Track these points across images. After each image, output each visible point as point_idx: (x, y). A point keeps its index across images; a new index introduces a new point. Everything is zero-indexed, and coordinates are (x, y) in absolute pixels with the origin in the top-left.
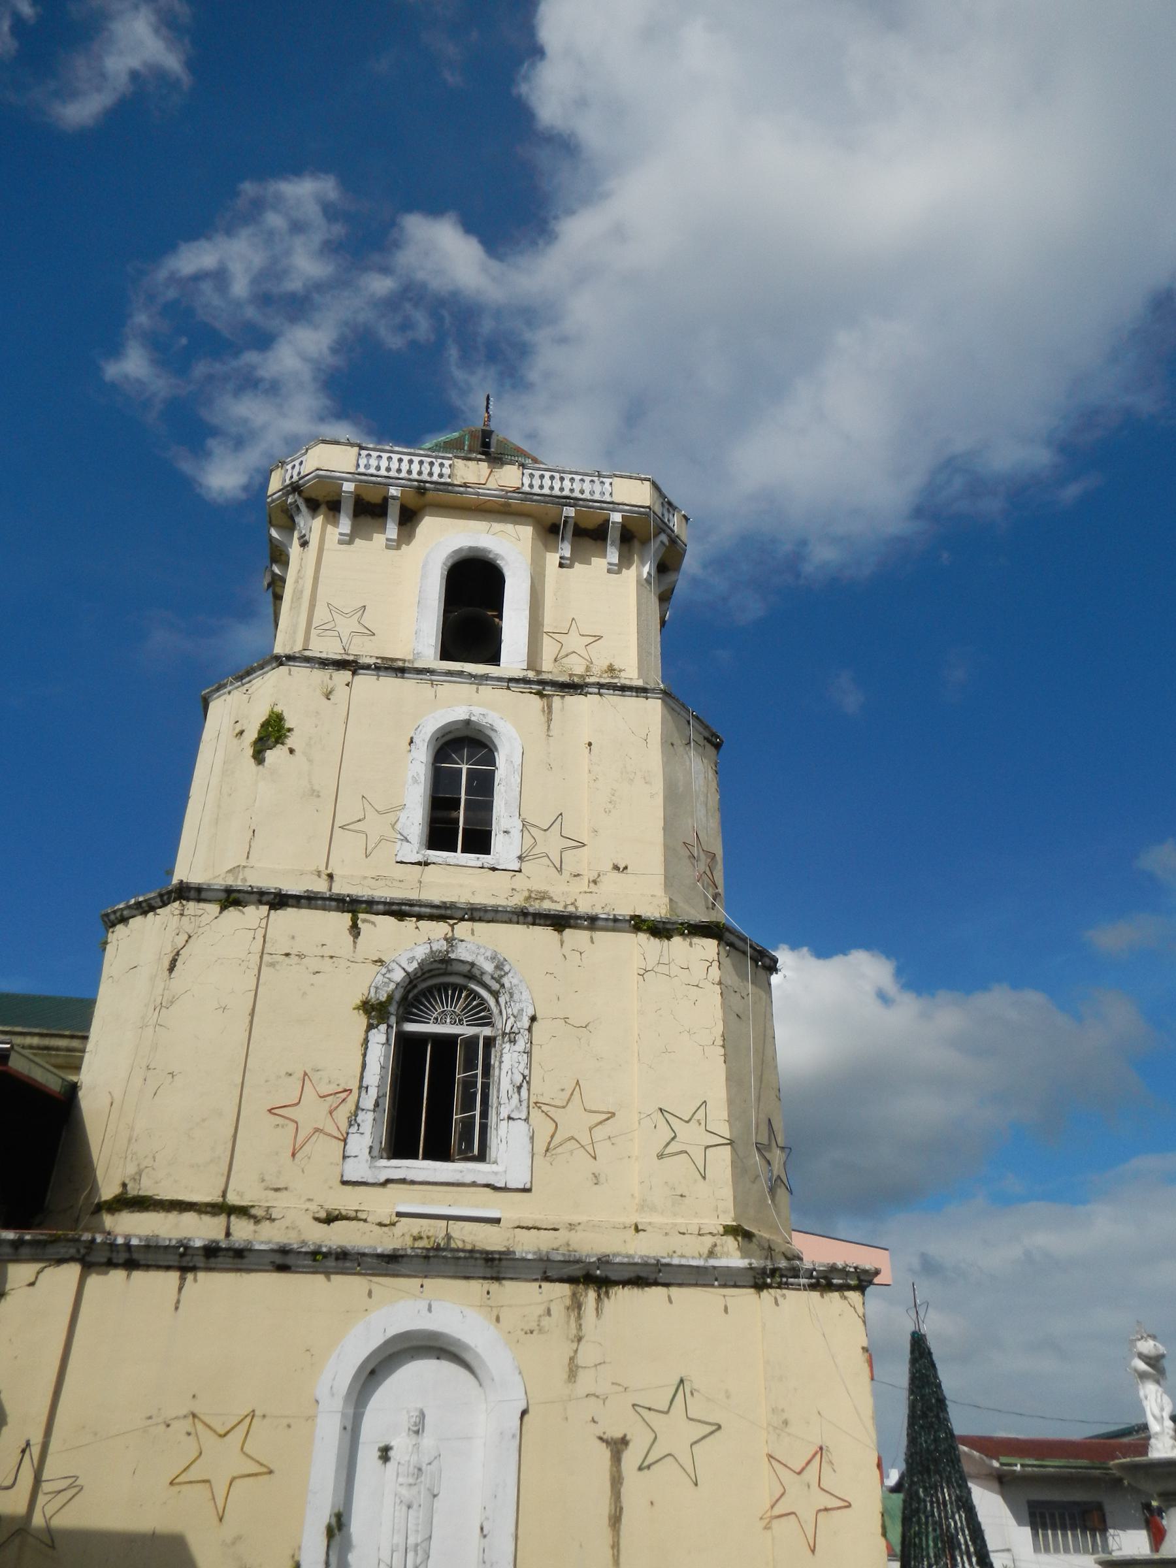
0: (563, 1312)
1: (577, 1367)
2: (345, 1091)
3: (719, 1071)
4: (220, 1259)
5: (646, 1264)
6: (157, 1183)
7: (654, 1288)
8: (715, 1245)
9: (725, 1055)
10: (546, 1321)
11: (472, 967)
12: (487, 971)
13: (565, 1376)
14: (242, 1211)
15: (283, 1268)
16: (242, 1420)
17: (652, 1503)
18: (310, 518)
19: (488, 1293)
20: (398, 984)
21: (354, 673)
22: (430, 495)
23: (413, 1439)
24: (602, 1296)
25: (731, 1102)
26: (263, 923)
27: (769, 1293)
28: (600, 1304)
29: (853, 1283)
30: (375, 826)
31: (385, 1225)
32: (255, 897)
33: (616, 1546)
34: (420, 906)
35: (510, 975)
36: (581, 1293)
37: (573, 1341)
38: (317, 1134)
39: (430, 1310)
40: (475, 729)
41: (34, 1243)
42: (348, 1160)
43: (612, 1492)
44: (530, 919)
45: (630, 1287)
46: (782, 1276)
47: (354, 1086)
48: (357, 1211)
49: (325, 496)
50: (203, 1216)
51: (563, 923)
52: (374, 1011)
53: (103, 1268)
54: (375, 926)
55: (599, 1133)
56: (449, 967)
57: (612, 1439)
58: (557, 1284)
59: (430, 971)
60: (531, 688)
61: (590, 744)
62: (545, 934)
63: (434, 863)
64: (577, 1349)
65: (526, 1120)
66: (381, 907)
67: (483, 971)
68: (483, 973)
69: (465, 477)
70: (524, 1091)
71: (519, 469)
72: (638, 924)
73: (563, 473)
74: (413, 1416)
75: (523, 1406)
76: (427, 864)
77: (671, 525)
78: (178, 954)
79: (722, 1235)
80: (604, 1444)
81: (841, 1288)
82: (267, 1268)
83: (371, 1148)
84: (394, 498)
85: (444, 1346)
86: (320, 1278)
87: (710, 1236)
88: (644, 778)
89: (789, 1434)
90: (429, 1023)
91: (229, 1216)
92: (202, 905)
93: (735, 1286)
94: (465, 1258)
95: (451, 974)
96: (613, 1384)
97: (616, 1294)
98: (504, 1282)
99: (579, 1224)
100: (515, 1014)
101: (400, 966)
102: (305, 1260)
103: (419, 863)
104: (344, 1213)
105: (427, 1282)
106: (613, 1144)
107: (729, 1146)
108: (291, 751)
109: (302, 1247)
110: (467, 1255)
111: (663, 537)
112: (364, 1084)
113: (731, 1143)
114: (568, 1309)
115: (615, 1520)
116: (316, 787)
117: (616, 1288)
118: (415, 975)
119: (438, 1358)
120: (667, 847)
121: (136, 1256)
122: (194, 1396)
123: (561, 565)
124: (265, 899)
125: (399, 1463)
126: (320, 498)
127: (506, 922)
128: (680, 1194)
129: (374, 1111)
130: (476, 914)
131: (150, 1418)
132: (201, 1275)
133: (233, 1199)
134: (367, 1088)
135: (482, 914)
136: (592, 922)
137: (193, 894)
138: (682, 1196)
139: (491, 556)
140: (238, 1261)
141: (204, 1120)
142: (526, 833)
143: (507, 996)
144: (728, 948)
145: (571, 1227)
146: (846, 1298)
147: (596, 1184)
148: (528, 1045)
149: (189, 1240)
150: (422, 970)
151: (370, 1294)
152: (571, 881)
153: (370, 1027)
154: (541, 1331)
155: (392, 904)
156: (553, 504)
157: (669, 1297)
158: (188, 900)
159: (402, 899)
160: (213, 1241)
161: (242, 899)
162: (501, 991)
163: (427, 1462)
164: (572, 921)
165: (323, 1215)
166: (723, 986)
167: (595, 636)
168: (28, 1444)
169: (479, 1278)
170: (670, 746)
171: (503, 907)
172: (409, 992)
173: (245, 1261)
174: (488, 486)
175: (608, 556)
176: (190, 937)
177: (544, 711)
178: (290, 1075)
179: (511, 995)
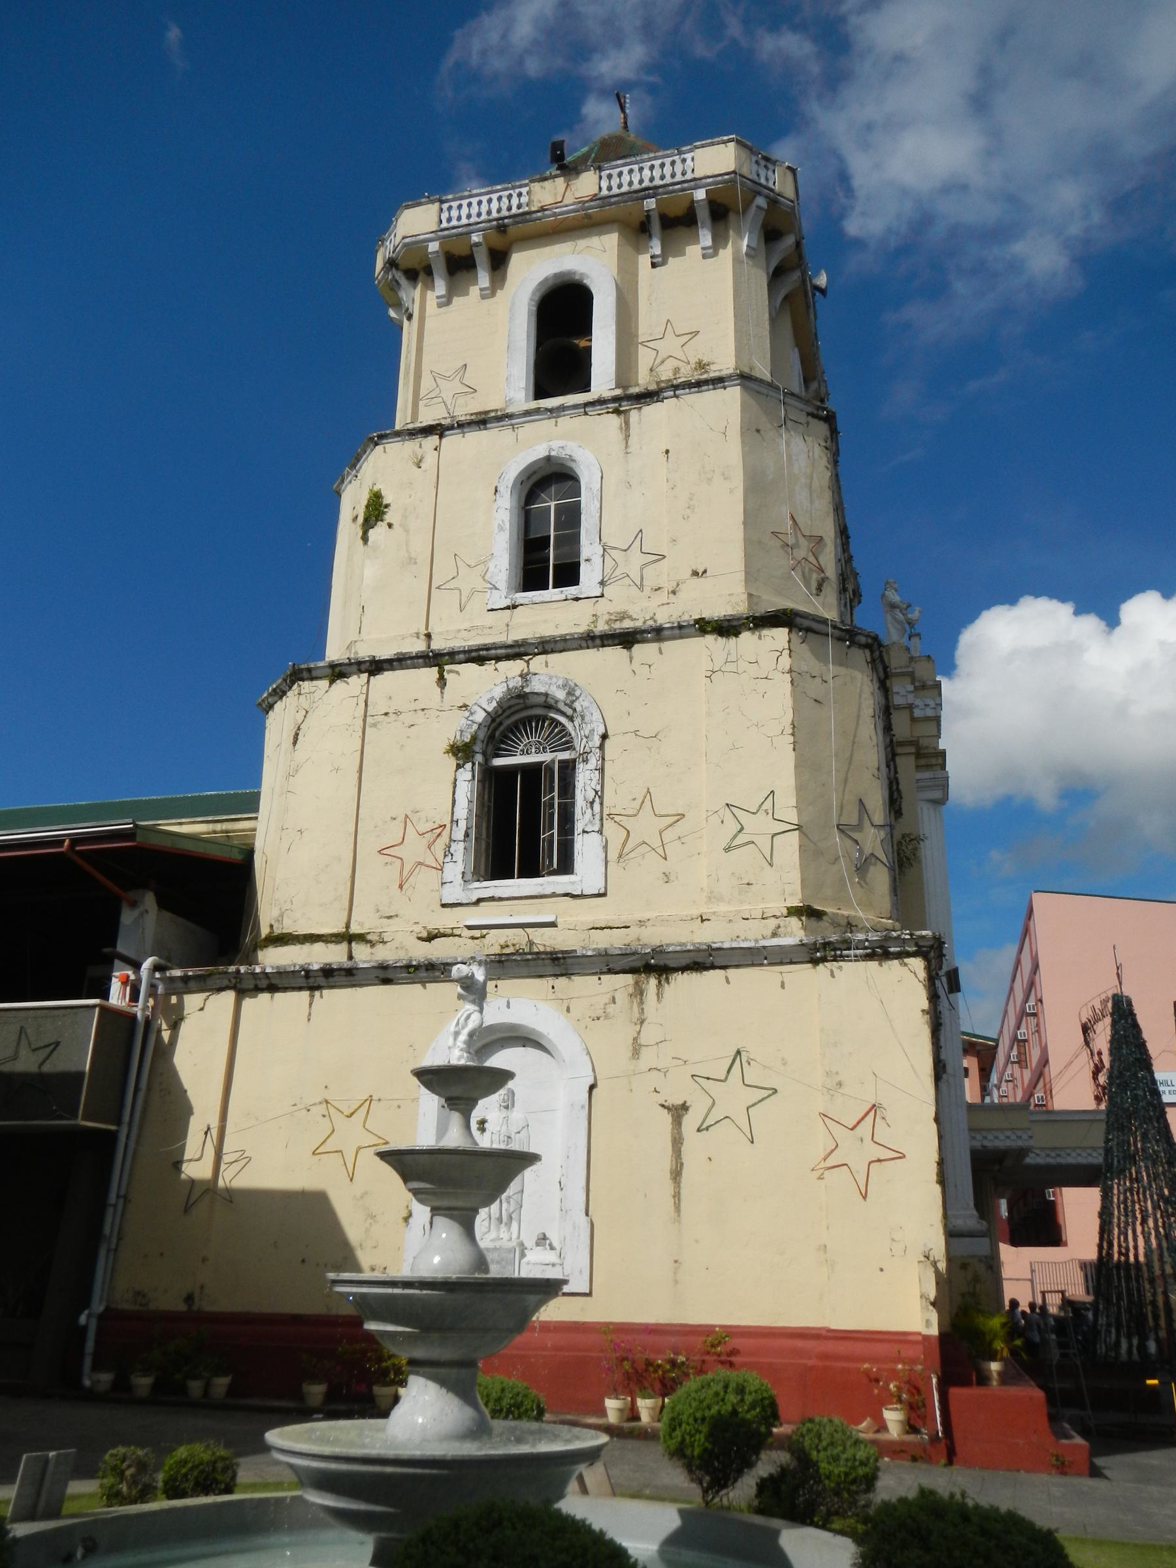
0: (627, 999)
1: (640, 1045)
2: (441, 826)
3: (786, 759)
4: (336, 979)
5: (698, 951)
6: (295, 921)
7: (711, 971)
8: (779, 927)
9: (794, 742)
10: (611, 1009)
11: (547, 697)
14: (361, 938)
15: (387, 981)
16: (363, 1104)
17: (710, 1159)
18: (412, 289)
19: (553, 987)
20: (480, 724)
21: (441, 436)
22: (511, 230)
23: (504, 1113)
25: (800, 788)
26: (364, 691)
27: (826, 967)
29: (912, 949)
30: (469, 580)
31: (477, 938)
32: (355, 668)
33: (677, 1196)
34: (496, 648)
35: (581, 699)
37: (636, 1024)
38: (419, 866)
39: (508, 1006)
40: (557, 464)
41: (197, 978)
42: (444, 885)
43: (673, 1150)
44: (598, 642)
45: (689, 972)
46: (835, 949)
47: (447, 821)
48: (452, 929)
49: (419, 263)
50: (329, 945)
51: (630, 639)
52: (461, 752)
53: (254, 992)
54: (459, 674)
55: (668, 836)
56: (527, 701)
57: (673, 1105)
58: (621, 975)
59: (510, 707)
60: (608, 408)
61: (667, 452)
62: (615, 654)
63: (521, 605)
64: (640, 1031)
65: (600, 832)
66: (462, 656)
68: (557, 702)
69: (541, 200)
70: (597, 806)
71: (595, 173)
72: (704, 627)
73: (641, 163)
75: (591, 1081)
76: (515, 607)
77: (771, 185)
78: (299, 729)
79: (786, 917)
80: (666, 1110)
81: (900, 956)
83: (463, 873)
84: (477, 245)
85: (526, 1035)
86: (419, 986)
87: (773, 919)
88: (723, 475)
89: (843, 1094)
90: (516, 755)
91: (350, 943)
92: (315, 683)
93: (791, 963)
94: (535, 959)
95: (532, 707)
96: (673, 1058)
97: (675, 979)
98: (573, 977)
99: (649, 920)
100: (587, 735)
101: (481, 707)
103: (508, 608)
104: (442, 931)
105: (499, 982)
107: (797, 831)
108: (390, 526)
109: (396, 963)
110: (534, 956)
111: (761, 201)
112: (455, 819)
113: (799, 828)
114: (631, 995)
115: (677, 1174)
116: (413, 555)
117: (676, 974)
118: (496, 713)
120: (747, 541)
121: (274, 981)
122: (326, 1087)
123: (654, 265)
124: (363, 667)
126: (416, 266)
127: (576, 649)
128: (746, 882)
129: (464, 841)
130: (547, 646)
131: (295, 1105)
132: (325, 992)
133: (355, 929)
134: (457, 822)
135: (552, 646)
136: (658, 633)
137: (305, 675)
138: (748, 884)
139: (577, 277)
140: (351, 978)
141: (327, 866)
142: (607, 556)
143: (579, 719)
144: (801, 633)
145: (641, 923)
146: (906, 965)
148: (600, 762)
149: (309, 964)
150: (502, 707)
152: (652, 596)
153: (459, 767)
154: (607, 1017)
155: (470, 651)
156: (632, 201)
157: (727, 979)
158: (303, 680)
159: (479, 645)
160: (327, 964)
161: (344, 671)
163: (516, 1131)
164: (638, 636)
165: (425, 934)
166: (794, 674)
167: (691, 333)
168: (209, 1129)
170: (756, 433)
171: (571, 634)
172: (495, 729)
173: (356, 978)
174: (566, 202)
175: (701, 240)
176: (307, 712)
177: (621, 428)
178: (395, 819)
179: (583, 718)
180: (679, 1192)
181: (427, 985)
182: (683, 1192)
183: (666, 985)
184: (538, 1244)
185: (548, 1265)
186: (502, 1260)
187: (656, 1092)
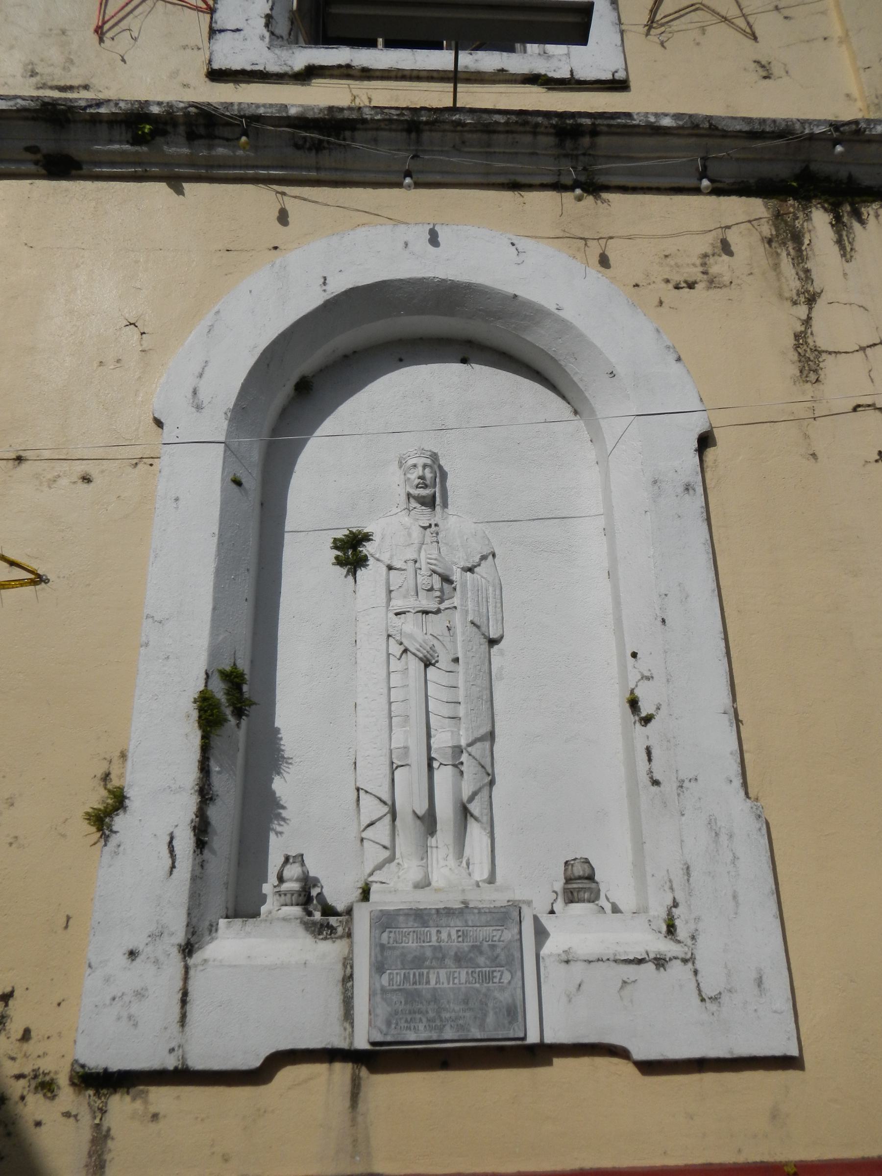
0: (761, 250)
1: (818, 352)
10: (720, 266)
13: (794, 370)
23: (423, 516)
24: (845, 219)
28: (844, 233)
36: (794, 214)
37: (795, 303)
39: (434, 239)
42: (219, 36)
58: (734, 198)
74: (415, 466)
82: (24, 168)
83: (269, 18)
86: (161, 189)
98: (605, 195)
102: (111, 142)
106: (786, 18)
114: (770, 242)
119: (464, 361)
125: (390, 568)
147: (765, 78)
151: (283, 218)
154: (713, 283)
169: (543, 187)
181: (186, 186)
183: (856, 225)
184: (571, 897)
185: (640, 961)
186: (477, 949)
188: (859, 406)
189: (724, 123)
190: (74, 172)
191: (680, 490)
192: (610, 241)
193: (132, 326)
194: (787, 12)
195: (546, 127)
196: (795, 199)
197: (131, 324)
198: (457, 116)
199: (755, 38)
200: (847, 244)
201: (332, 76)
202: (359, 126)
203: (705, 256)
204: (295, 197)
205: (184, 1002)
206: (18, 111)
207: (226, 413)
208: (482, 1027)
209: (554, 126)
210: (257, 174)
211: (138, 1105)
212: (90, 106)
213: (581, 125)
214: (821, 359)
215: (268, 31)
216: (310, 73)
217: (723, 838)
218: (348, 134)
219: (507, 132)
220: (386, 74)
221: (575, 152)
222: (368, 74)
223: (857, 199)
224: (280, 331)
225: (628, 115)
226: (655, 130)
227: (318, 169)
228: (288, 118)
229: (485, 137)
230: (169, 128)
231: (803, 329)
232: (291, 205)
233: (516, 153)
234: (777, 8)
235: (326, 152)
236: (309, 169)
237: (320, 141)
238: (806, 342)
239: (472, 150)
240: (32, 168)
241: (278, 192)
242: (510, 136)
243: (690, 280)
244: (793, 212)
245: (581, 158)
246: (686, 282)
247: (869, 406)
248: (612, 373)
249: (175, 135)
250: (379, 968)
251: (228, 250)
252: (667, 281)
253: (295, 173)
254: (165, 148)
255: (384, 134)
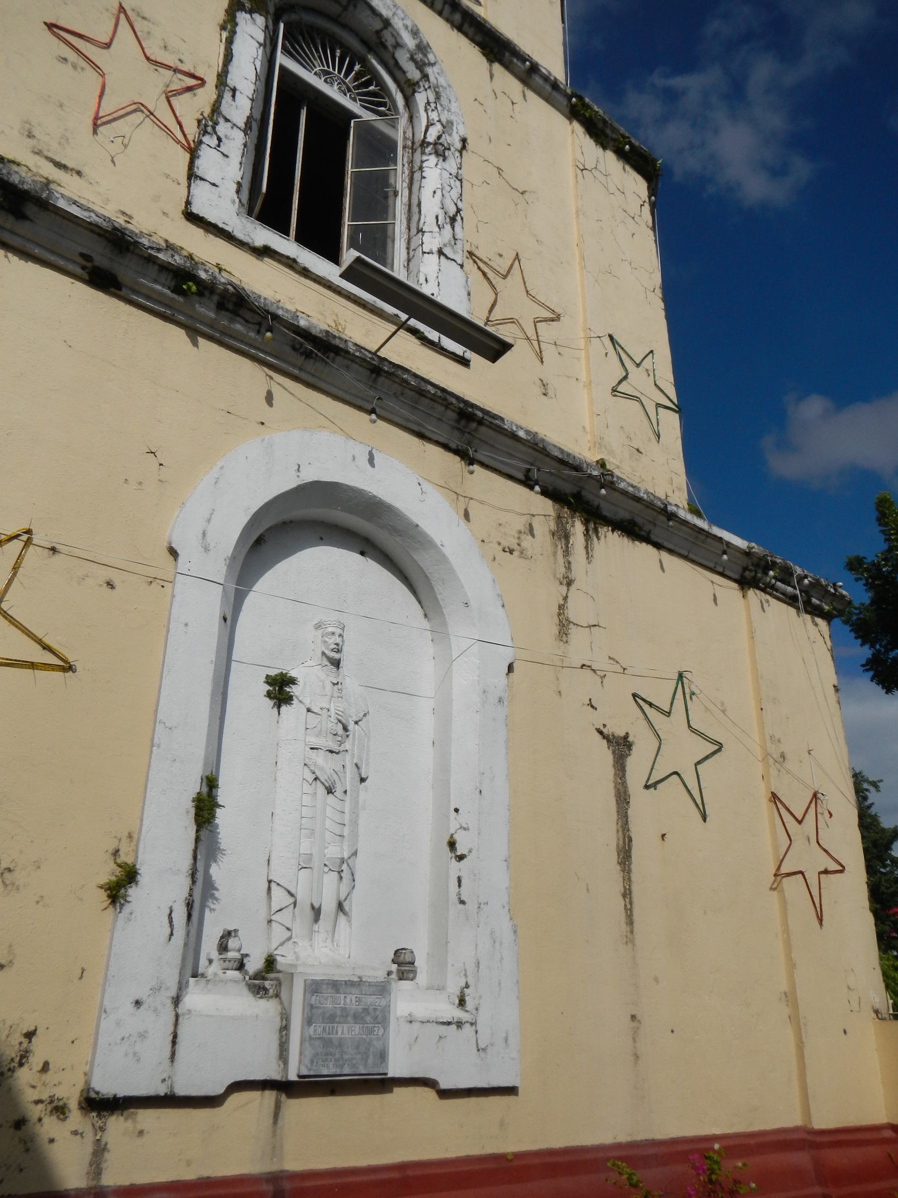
0: (548, 537)
7: (644, 544)
10: (527, 541)
12: (406, 45)
24: (591, 532)
33: (627, 894)
37: (561, 584)
38: (138, 117)
39: (371, 461)
51: (496, 50)
57: (613, 735)
67: (399, 40)
74: (333, 633)
80: (605, 741)
82: (71, 267)
86: (179, 334)
90: (310, 71)
93: (722, 574)
95: (344, 26)
97: (605, 537)
102: (155, 281)
106: (559, 353)
114: (553, 535)
115: (625, 855)
117: (605, 529)
119: (362, 553)
125: (309, 710)
162: (421, 83)
169: (438, 443)
173: (23, 227)
180: (630, 889)
181: (201, 341)
182: (635, 888)
185: (449, 1023)
186: (366, 1010)
187: (592, 707)
188: (584, 665)
189: (550, 447)
190: (113, 290)
191: (497, 701)
192: (471, 501)
193: (153, 454)
194: (561, 350)
195: (455, 407)
196: (568, 509)
197: (152, 453)
198: (406, 376)
199: (542, 362)
200: (590, 551)
201: (279, 262)
202: (342, 354)
203: (520, 532)
204: (279, 384)
205: (174, 1043)
206: (90, 223)
207: (225, 560)
208: (365, 1065)
209: (460, 408)
210: (257, 354)
211: (129, 1124)
212: (152, 248)
213: (475, 415)
214: (570, 627)
215: (238, 197)
216: (265, 252)
217: (497, 944)
218: (332, 355)
219: (431, 399)
220: (318, 279)
221: (464, 429)
222: (306, 273)
223: (598, 521)
224: (266, 500)
225: (502, 419)
226: (514, 436)
227: (301, 369)
228: (298, 327)
229: (417, 396)
230: (206, 293)
231: (563, 603)
232: (277, 392)
233: (430, 415)
234: (555, 344)
235: (312, 361)
236: (294, 366)
237: (311, 351)
238: (564, 613)
239: (405, 401)
240: (78, 271)
241: (267, 375)
242: (432, 403)
243: (512, 547)
244: (566, 518)
245: (466, 435)
246: (509, 548)
247: (589, 666)
248: (467, 604)
249: (208, 299)
250: (308, 1021)
251: (228, 412)
252: (499, 544)
253: (284, 366)
254: (197, 306)
255: (355, 366)
